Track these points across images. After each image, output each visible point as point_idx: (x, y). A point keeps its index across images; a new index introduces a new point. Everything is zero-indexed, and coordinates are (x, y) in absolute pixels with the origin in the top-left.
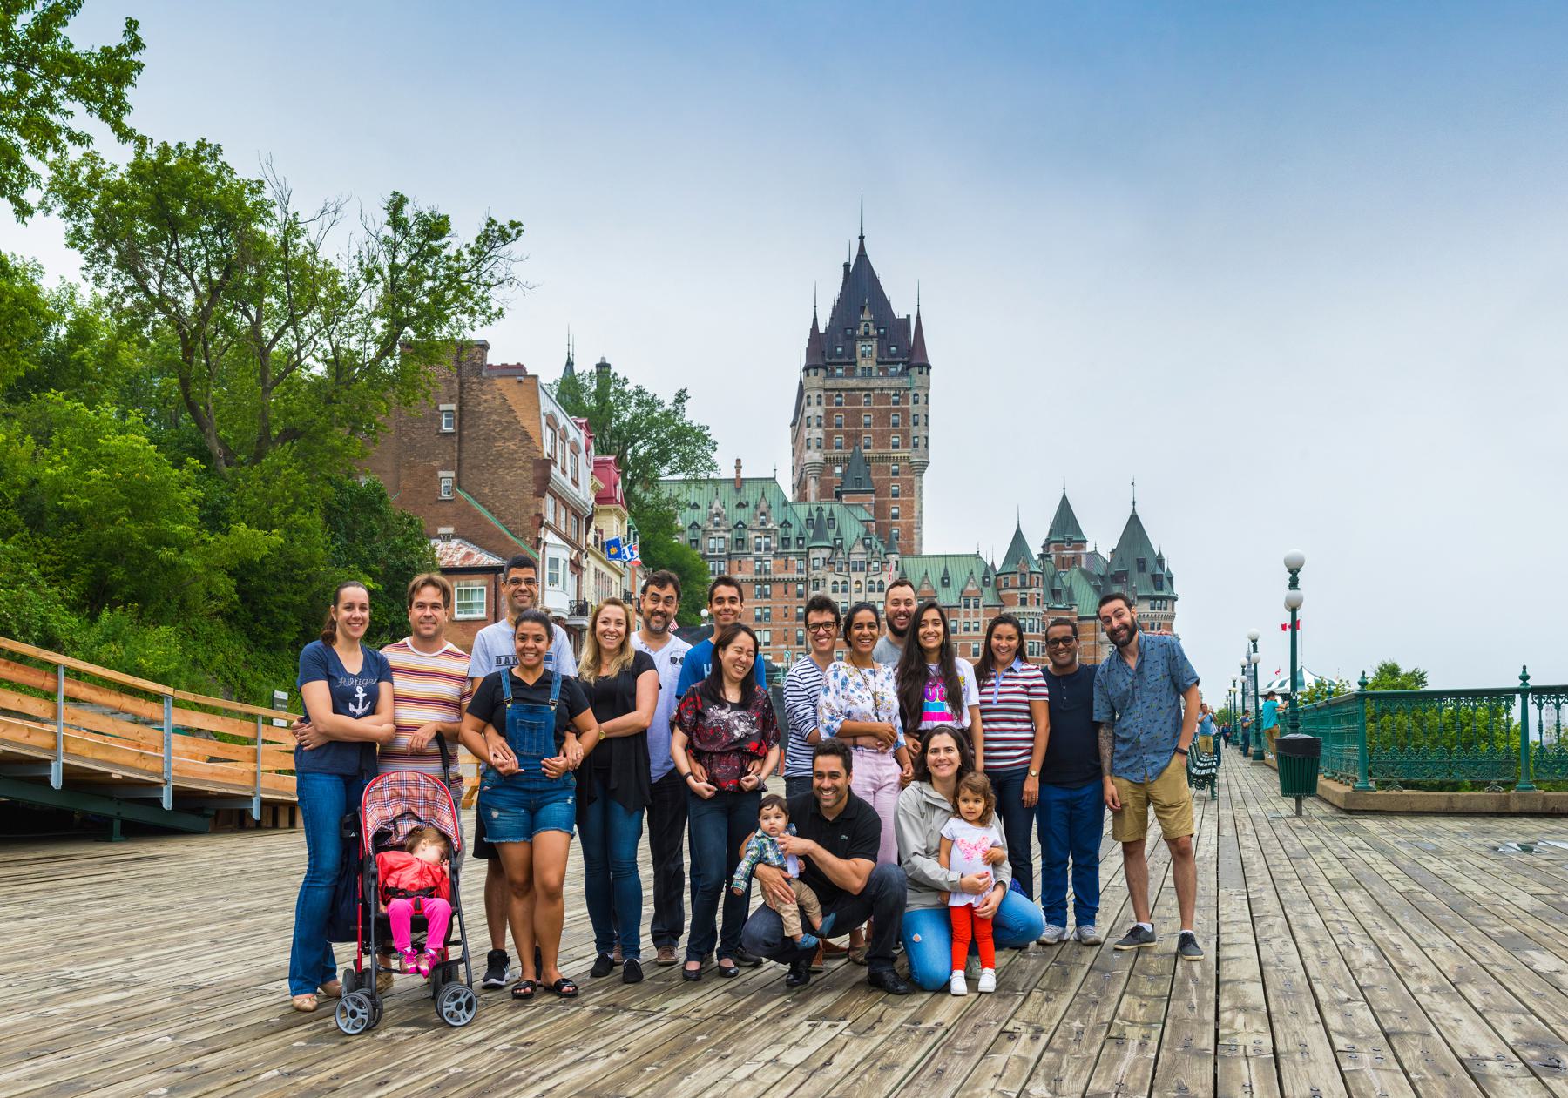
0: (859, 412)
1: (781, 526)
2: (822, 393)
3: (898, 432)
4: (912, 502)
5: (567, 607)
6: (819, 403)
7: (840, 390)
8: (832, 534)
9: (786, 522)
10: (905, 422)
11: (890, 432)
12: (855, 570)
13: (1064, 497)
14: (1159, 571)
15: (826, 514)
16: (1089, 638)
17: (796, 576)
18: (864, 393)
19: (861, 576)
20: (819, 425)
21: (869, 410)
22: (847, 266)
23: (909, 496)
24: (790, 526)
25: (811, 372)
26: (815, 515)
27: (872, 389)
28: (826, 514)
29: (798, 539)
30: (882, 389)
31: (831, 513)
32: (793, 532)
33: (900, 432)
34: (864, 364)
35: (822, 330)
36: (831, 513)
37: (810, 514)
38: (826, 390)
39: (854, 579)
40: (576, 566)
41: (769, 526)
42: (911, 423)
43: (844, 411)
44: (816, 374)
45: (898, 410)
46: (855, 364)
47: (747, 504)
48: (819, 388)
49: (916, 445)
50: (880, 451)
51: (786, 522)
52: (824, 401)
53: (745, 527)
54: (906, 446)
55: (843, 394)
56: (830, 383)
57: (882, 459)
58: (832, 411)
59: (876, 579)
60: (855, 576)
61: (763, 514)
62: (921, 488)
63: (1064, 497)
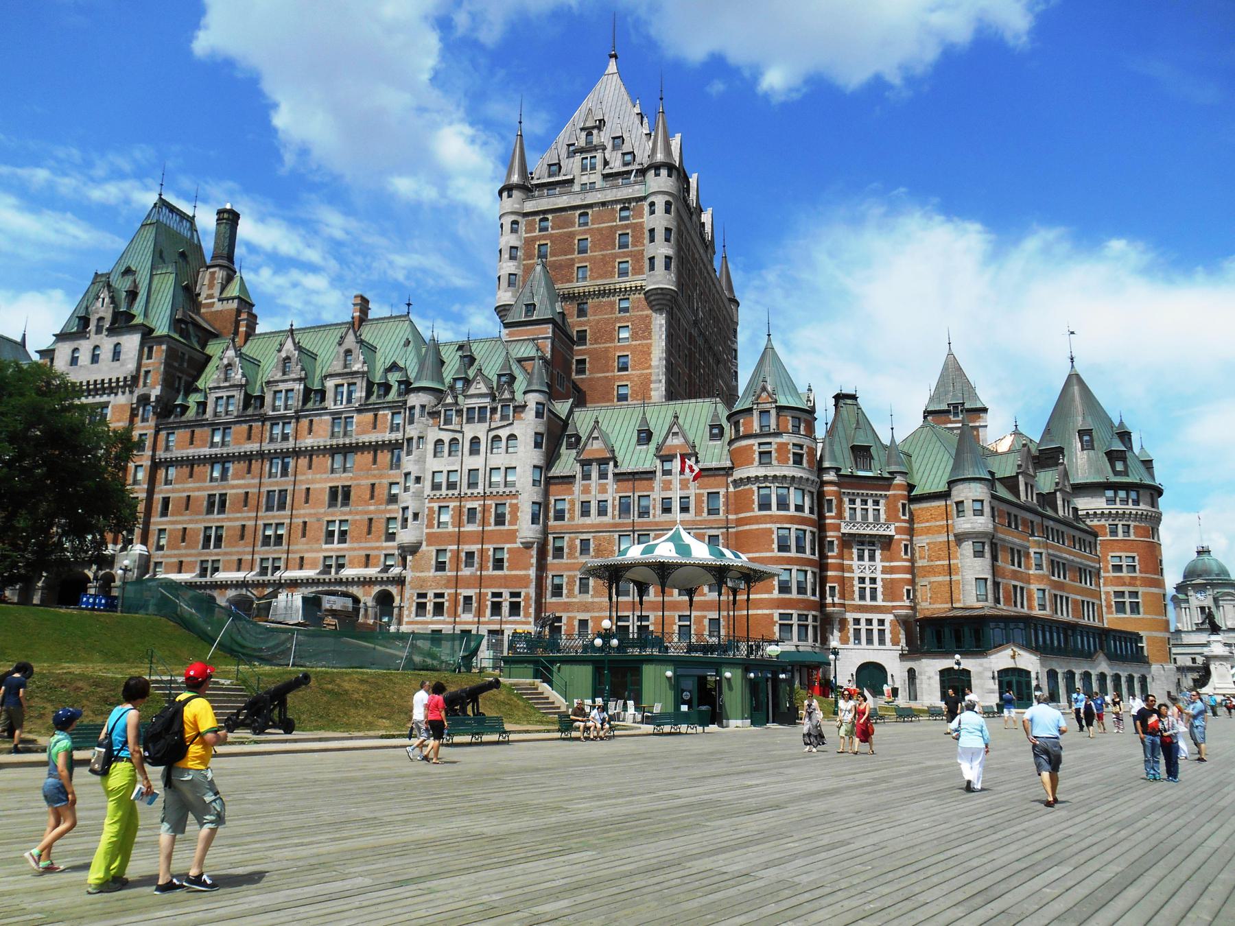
0: (571, 235)
3: (626, 255)
4: (651, 344)
6: (513, 231)
10: (638, 240)
11: (615, 256)
12: (470, 420)
13: (950, 354)
14: (1118, 446)
16: (937, 531)
17: (388, 436)
18: (579, 212)
19: (479, 430)
20: (512, 258)
21: (585, 232)
23: (644, 338)
25: (505, 194)
27: (590, 206)
33: (630, 254)
34: (585, 179)
38: (526, 215)
39: (469, 435)
42: (646, 241)
43: (551, 237)
45: (627, 226)
46: (573, 179)
48: (512, 213)
49: (652, 268)
52: (522, 227)
54: (638, 271)
55: (550, 217)
56: (530, 206)
57: (603, 293)
58: (534, 239)
59: (504, 433)
60: (470, 431)
63: (950, 354)
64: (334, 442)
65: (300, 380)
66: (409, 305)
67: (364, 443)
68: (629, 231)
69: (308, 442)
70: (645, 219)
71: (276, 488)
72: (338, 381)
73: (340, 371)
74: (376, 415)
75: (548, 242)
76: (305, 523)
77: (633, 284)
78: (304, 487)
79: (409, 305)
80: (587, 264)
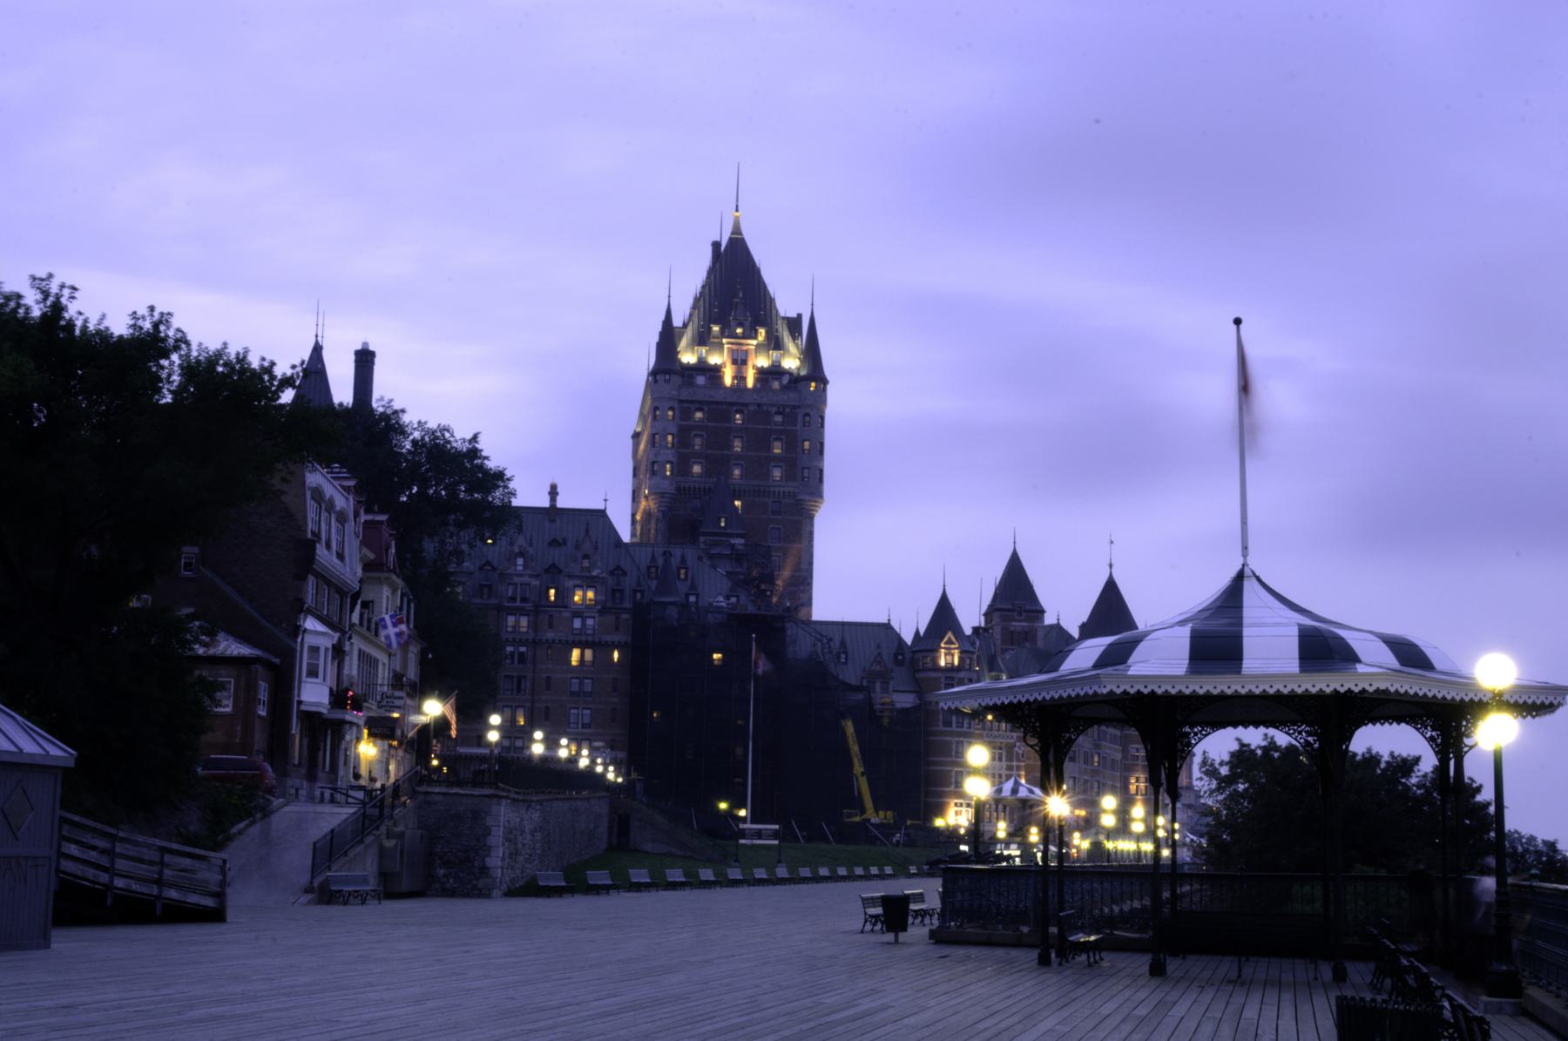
1: (612, 573)
2: (676, 405)
5: (325, 700)
7: (700, 402)
8: (683, 588)
9: (618, 568)
15: (675, 561)
22: (716, 245)
24: (625, 573)
26: (660, 562)
27: (746, 405)
28: (675, 561)
29: (635, 591)
30: (759, 405)
31: (683, 560)
32: (628, 583)
35: (677, 322)
36: (683, 560)
37: (653, 558)
38: (681, 401)
40: (338, 652)
41: (594, 574)
44: (668, 381)
47: (565, 542)
50: (755, 482)
51: (618, 568)
53: (560, 571)
55: (706, 408)
56: (686, 394)
61: (586, 557)
62: (811, 533)
64: (577, 638)
65: (537, 576)
66: (606, 500)
67: (606, 642)
68: (783, 437)
69: (550, 635)
70: (799, 427)
71: (515, 674)
72: (578, 582)
73: (578, 574)
74: (617, 618)
75: (703, 433)
76: (547, 708)
77: (787, 489)
78: (545, 675)
79: (606, 500)
80: (743, 463)
